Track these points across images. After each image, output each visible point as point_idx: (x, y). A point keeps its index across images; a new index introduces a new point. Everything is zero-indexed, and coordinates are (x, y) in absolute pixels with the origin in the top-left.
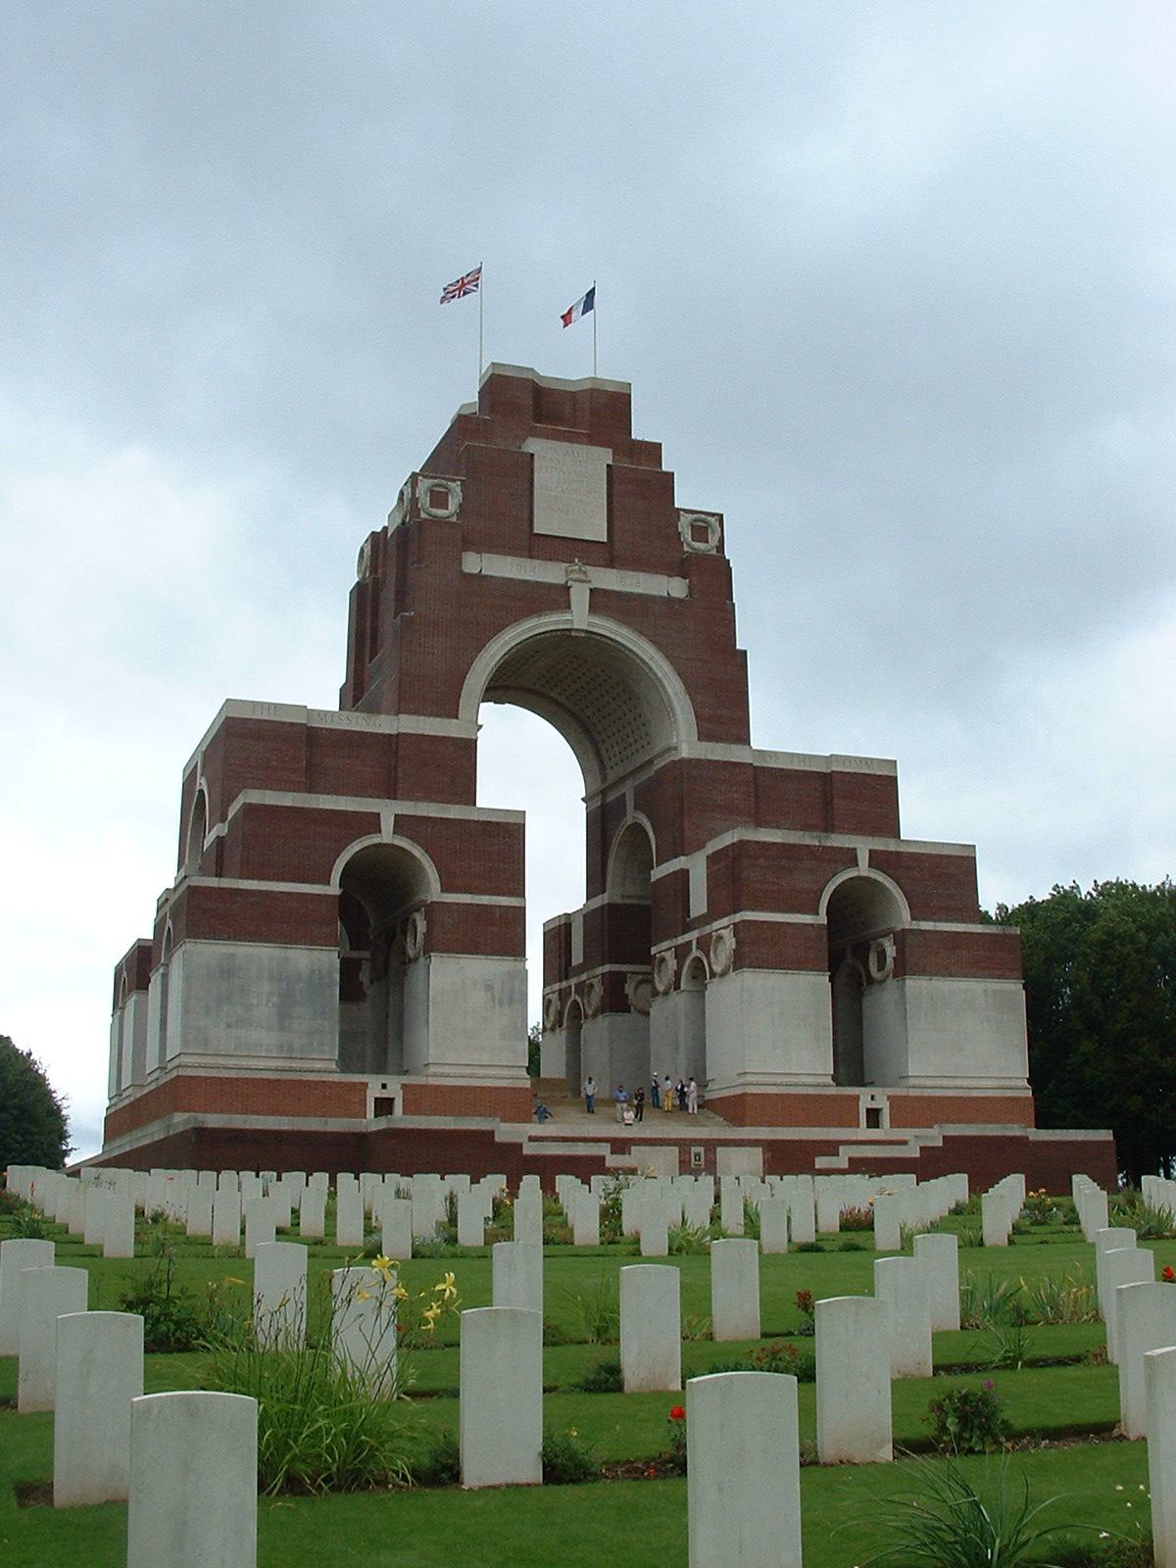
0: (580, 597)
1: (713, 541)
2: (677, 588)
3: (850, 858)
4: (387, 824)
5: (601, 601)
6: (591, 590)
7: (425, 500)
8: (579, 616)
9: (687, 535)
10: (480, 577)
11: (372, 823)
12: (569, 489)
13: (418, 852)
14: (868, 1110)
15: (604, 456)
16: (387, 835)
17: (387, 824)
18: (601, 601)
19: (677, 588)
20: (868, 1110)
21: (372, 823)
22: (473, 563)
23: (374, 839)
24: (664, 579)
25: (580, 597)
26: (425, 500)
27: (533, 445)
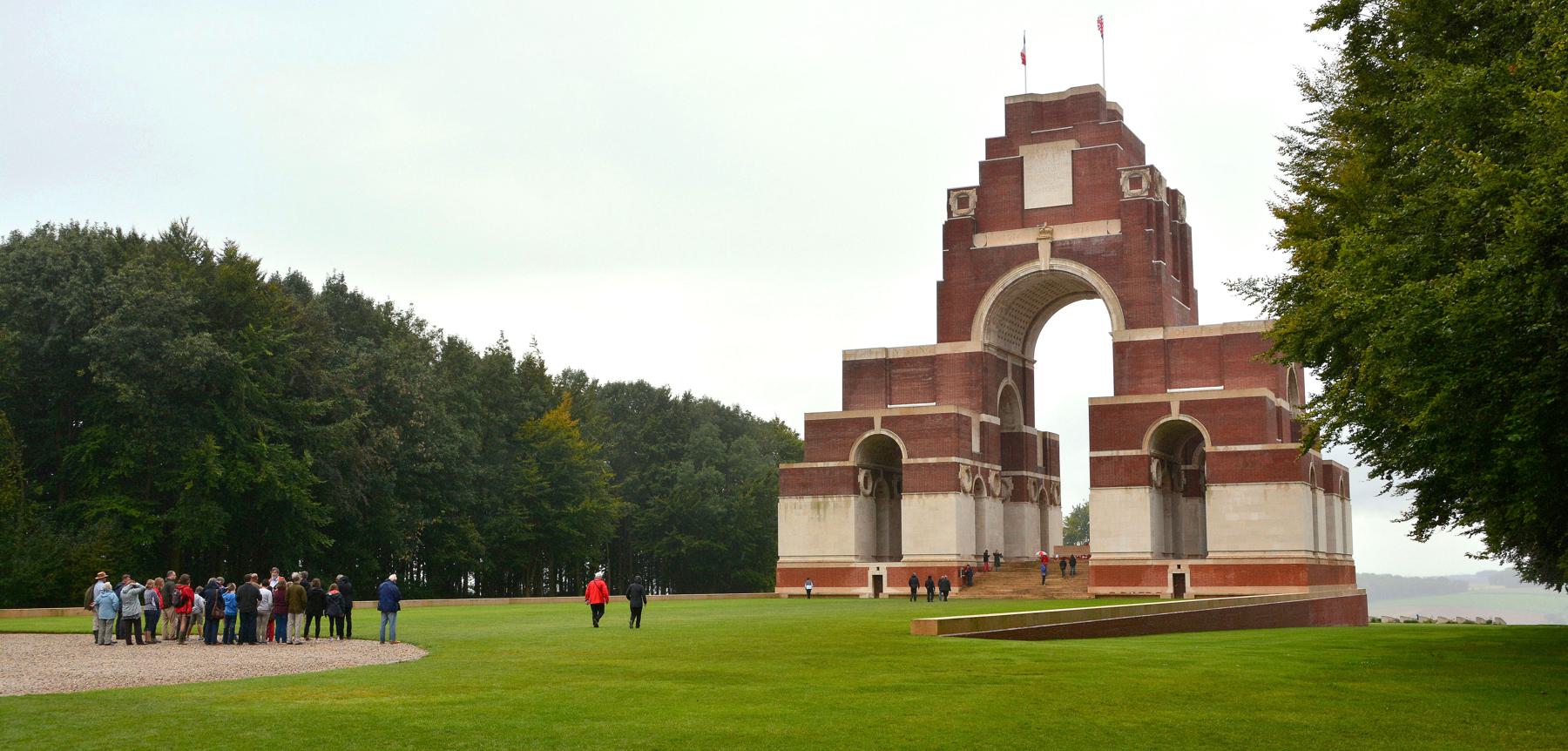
0: (1044, 249)
1: (1145, 184)
2: (1113, 228)
3: (1165, 408)
4: (877, 423)
5: (1060, 251)
6: (1053, 244)
7: (955, 207)
8: (1044, 262)
9: (1126, 187)
10: (985, 250)
11: (869, 423)
12: (1049, 178)
14: (1175, 575)
15: (1072, 145)
17: (877, 423)
18: (1060, 251)
19: (1113, 228)
20: (1175, 575)
21: (869, 423)
22: (982, 241)
24: (1103, 223)
25: (1044, 249)
26: (955, 207)
27: (1024, 151)
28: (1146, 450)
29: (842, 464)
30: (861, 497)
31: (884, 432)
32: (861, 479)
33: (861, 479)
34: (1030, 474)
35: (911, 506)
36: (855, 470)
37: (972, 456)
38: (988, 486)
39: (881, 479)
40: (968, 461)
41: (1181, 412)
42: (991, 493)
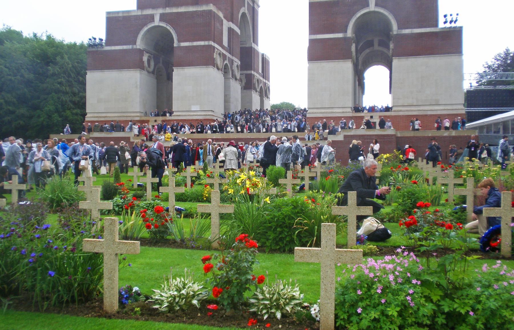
4: (157, 18)
13: (169, 28)
16: (157, 22)
17: (157, 18)
21: (152, 18)
23: (150, 26)
28: (350, 33)
29: (129, 47)
30: (146, 72)
31: (163, 24)
32: (145, 58)
33: (145, 58)
34: (255, 74)
35: (182, 77)
36: (141, 52)
37: (223, 47)
38: (232, 71)
39: (161, 65)
40: (220, 48)
41: (377, 5)
42: (234, 76)
